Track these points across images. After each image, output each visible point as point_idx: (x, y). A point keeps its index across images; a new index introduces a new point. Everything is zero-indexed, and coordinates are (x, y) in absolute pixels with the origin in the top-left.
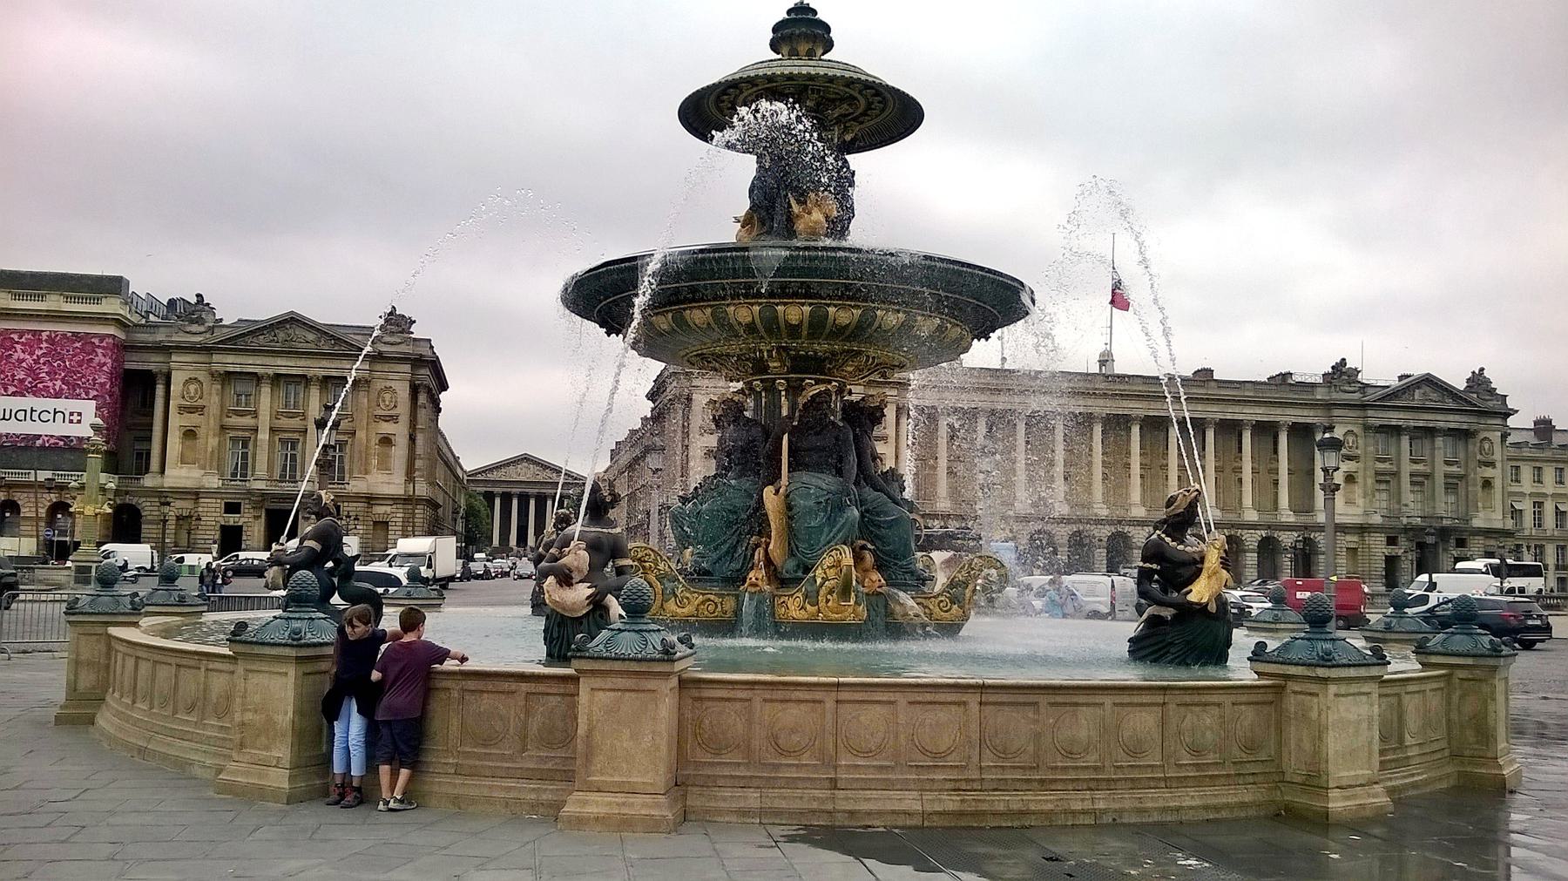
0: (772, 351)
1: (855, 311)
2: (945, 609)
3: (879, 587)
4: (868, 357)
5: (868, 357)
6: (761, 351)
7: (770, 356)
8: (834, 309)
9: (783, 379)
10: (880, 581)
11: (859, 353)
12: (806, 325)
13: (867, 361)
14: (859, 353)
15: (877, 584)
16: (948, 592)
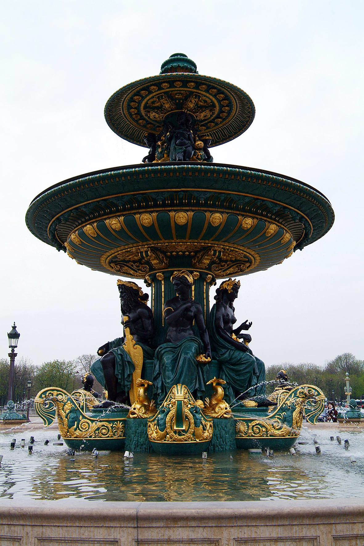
0: (148, 251)
1: (189, 213)
2: (277, 427)
3: (225, 414)
4: (215, 251)
5: (215, 251)
6: (141, 253)
7: (147, 255)
8: (174, 213)
9: (160, 272)
10: (226, 409)
11: (209, 248)
12: (156, 225)
13: (214, 255)
14: (209, 248)
15: (224, 411)
16: (280, 415)
